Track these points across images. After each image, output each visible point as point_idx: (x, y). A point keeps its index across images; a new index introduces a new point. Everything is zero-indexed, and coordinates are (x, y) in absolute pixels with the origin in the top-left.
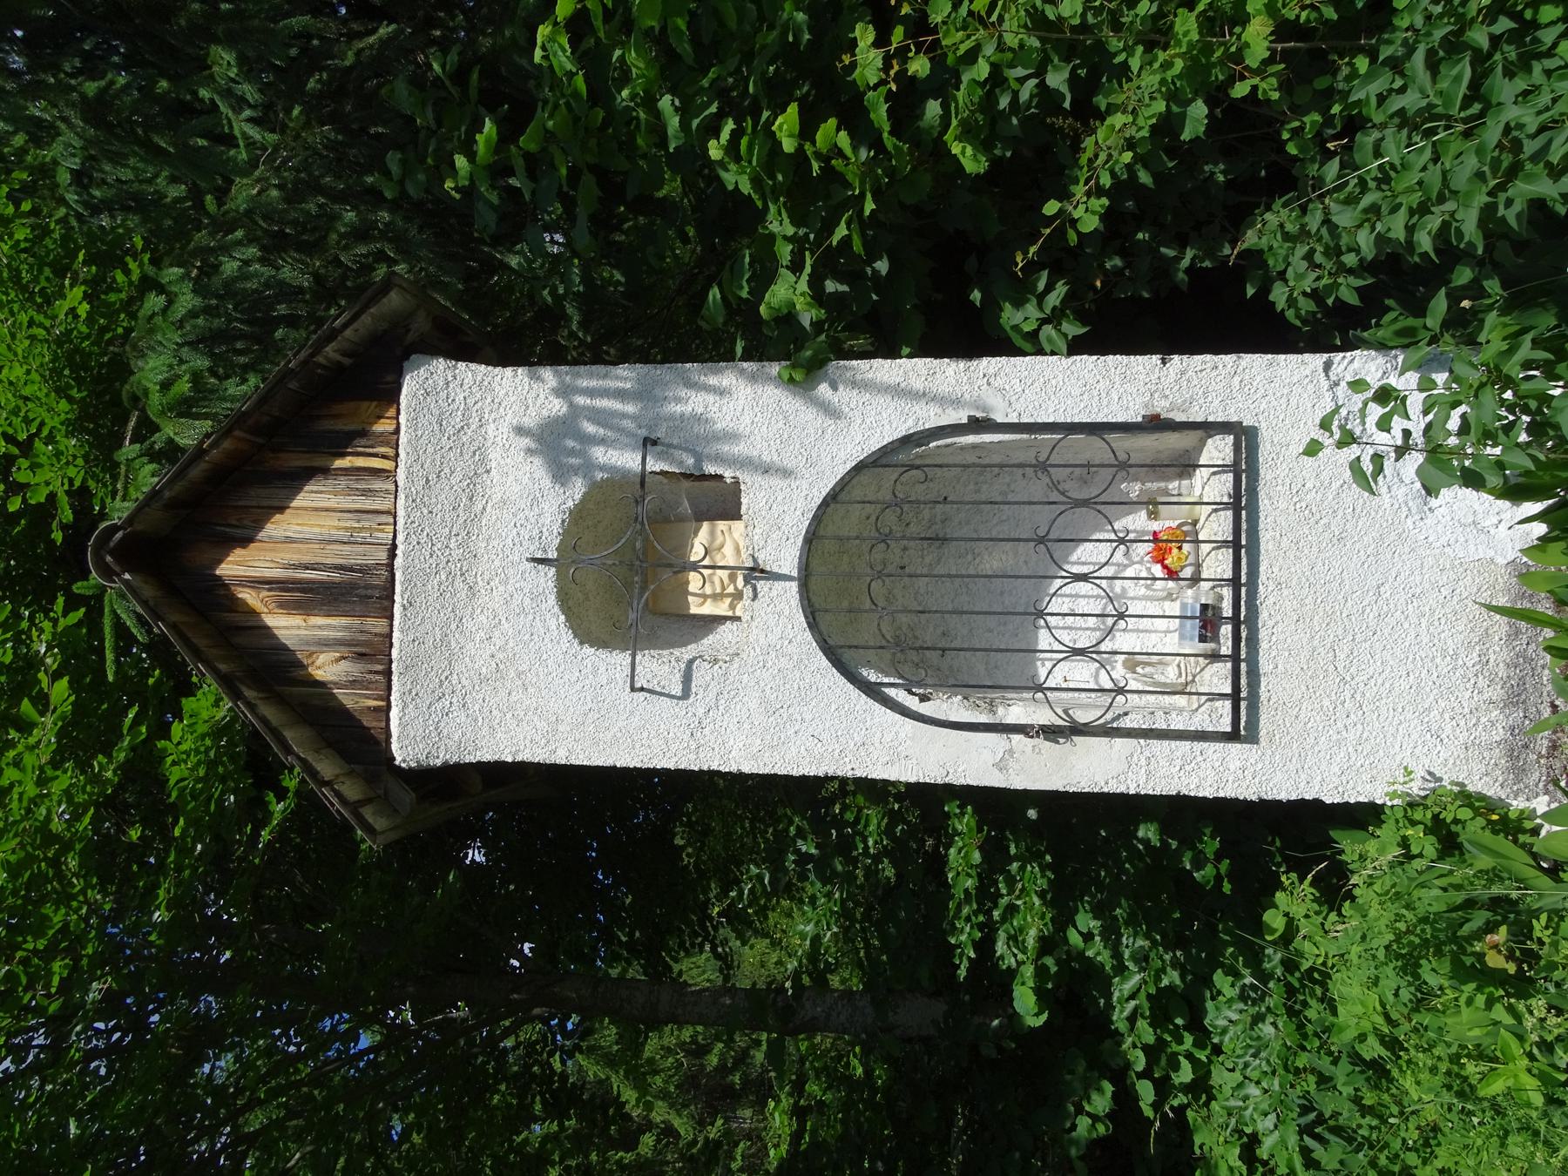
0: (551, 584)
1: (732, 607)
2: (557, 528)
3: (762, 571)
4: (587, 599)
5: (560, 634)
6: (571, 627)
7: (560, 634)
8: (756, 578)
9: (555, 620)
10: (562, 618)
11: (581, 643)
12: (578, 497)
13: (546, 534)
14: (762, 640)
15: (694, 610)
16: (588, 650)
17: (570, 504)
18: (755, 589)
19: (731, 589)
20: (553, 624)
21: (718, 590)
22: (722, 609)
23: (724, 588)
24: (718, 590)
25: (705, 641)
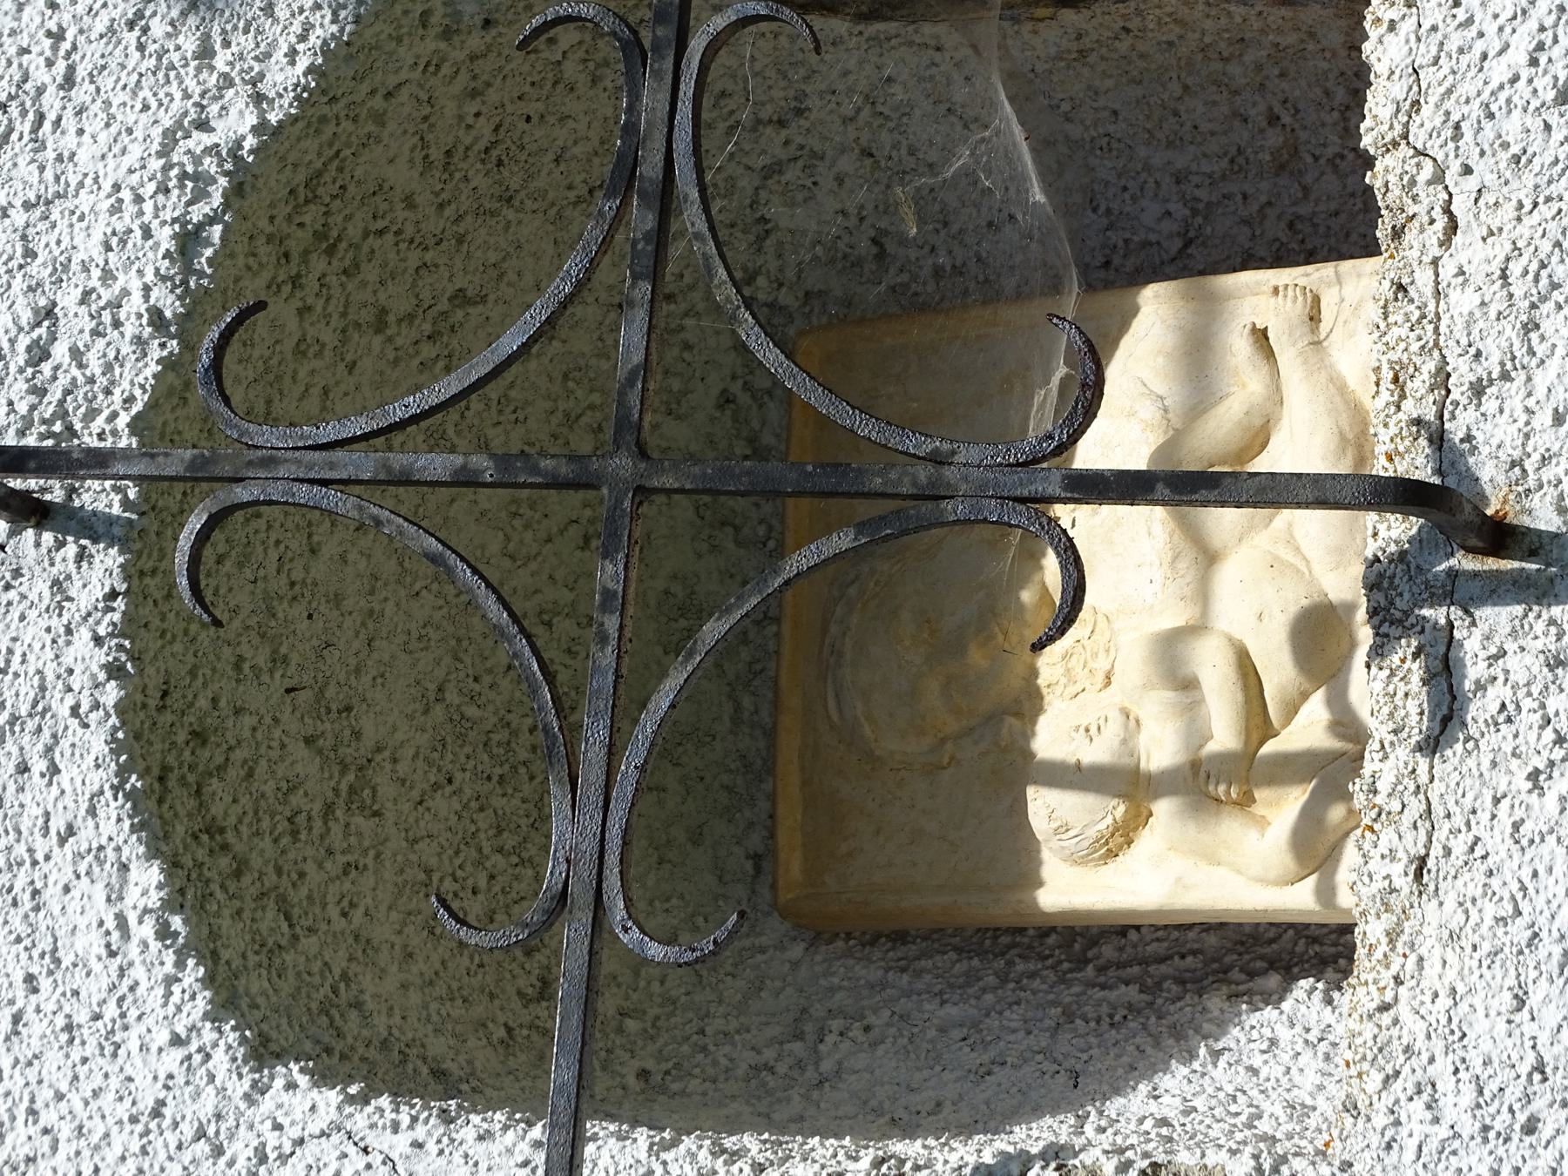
0: (86, 656)
1: (1315, 849)
2: (145, 283)
3: (1500, 536)
4: (361, 799)
5: (123, 993)
6: (206, 947)
7: (123, 993)
8: (1453, 590)
9: (102, 893)
10: (147, 879)
11: (263, 1053)
12: (285, 77)
13: (75, 322)
14: (1487, 1031)
15: (1067, 887)
16: (301, 1102)
17: (236, 123)
18: (1443, 671)
19: (1308, 730)
20: (80, 919)
21: (1224, 736)
22: (1234, 869)
23: (1258, 723)
24: (1224, 736)
25: (1133, 1105)
